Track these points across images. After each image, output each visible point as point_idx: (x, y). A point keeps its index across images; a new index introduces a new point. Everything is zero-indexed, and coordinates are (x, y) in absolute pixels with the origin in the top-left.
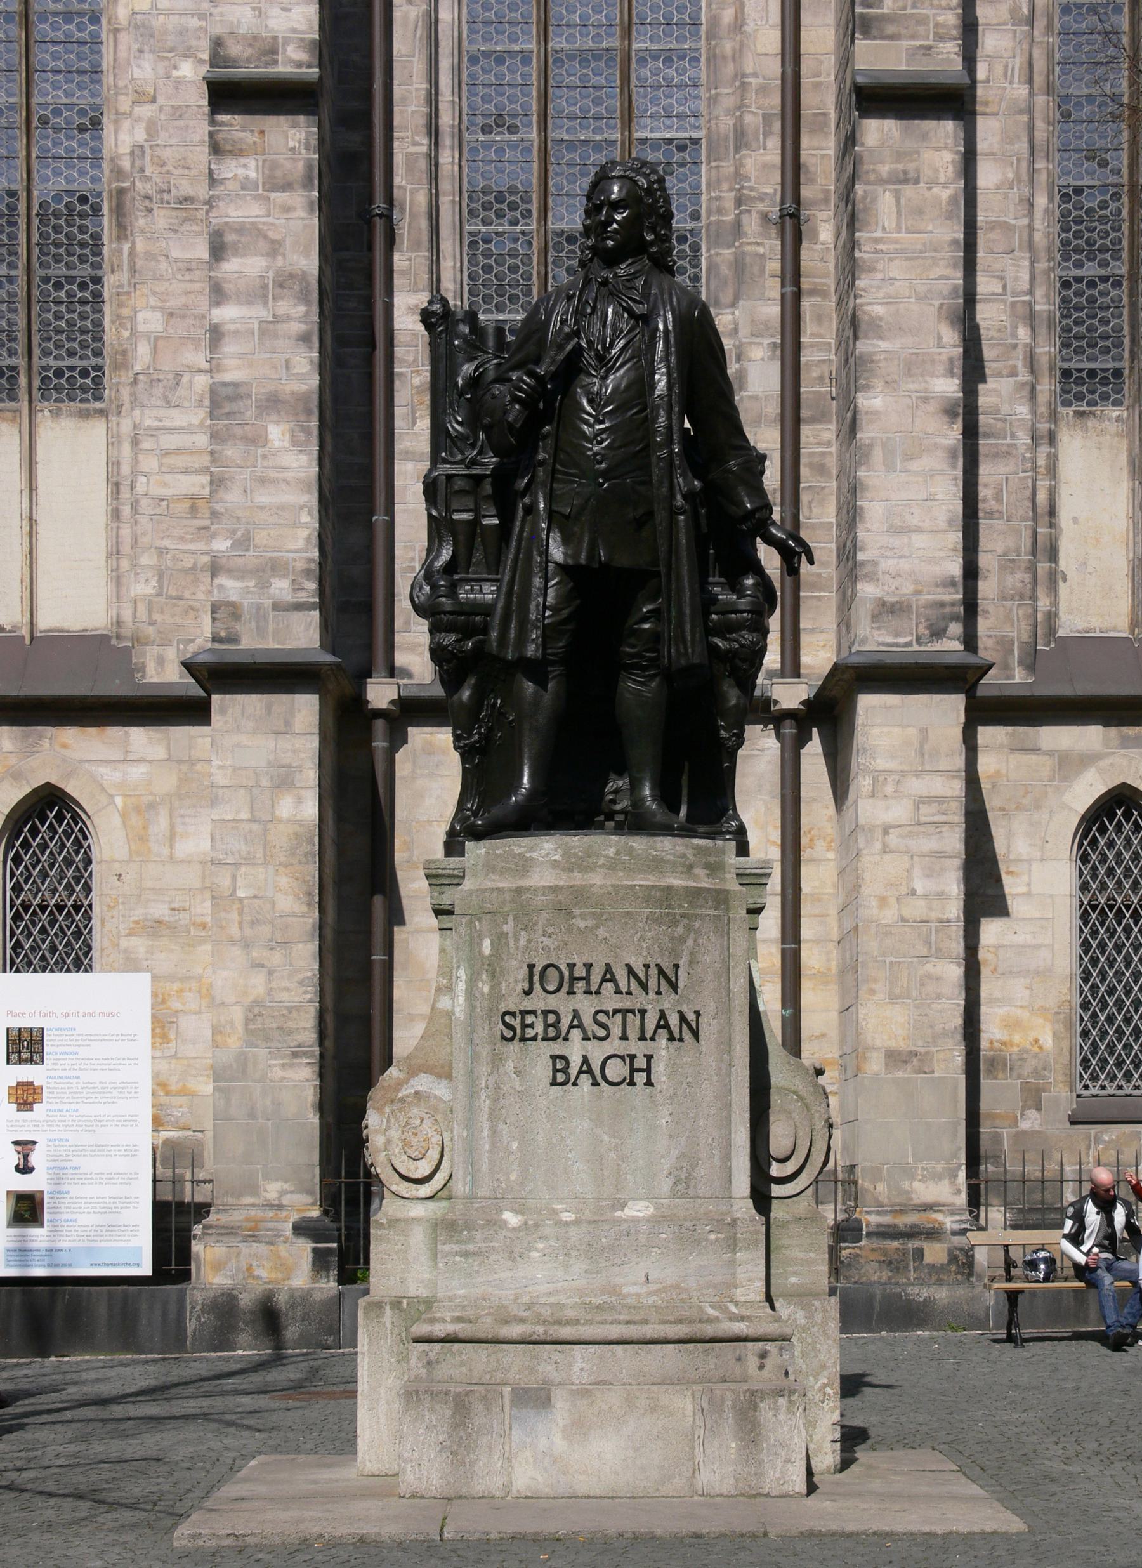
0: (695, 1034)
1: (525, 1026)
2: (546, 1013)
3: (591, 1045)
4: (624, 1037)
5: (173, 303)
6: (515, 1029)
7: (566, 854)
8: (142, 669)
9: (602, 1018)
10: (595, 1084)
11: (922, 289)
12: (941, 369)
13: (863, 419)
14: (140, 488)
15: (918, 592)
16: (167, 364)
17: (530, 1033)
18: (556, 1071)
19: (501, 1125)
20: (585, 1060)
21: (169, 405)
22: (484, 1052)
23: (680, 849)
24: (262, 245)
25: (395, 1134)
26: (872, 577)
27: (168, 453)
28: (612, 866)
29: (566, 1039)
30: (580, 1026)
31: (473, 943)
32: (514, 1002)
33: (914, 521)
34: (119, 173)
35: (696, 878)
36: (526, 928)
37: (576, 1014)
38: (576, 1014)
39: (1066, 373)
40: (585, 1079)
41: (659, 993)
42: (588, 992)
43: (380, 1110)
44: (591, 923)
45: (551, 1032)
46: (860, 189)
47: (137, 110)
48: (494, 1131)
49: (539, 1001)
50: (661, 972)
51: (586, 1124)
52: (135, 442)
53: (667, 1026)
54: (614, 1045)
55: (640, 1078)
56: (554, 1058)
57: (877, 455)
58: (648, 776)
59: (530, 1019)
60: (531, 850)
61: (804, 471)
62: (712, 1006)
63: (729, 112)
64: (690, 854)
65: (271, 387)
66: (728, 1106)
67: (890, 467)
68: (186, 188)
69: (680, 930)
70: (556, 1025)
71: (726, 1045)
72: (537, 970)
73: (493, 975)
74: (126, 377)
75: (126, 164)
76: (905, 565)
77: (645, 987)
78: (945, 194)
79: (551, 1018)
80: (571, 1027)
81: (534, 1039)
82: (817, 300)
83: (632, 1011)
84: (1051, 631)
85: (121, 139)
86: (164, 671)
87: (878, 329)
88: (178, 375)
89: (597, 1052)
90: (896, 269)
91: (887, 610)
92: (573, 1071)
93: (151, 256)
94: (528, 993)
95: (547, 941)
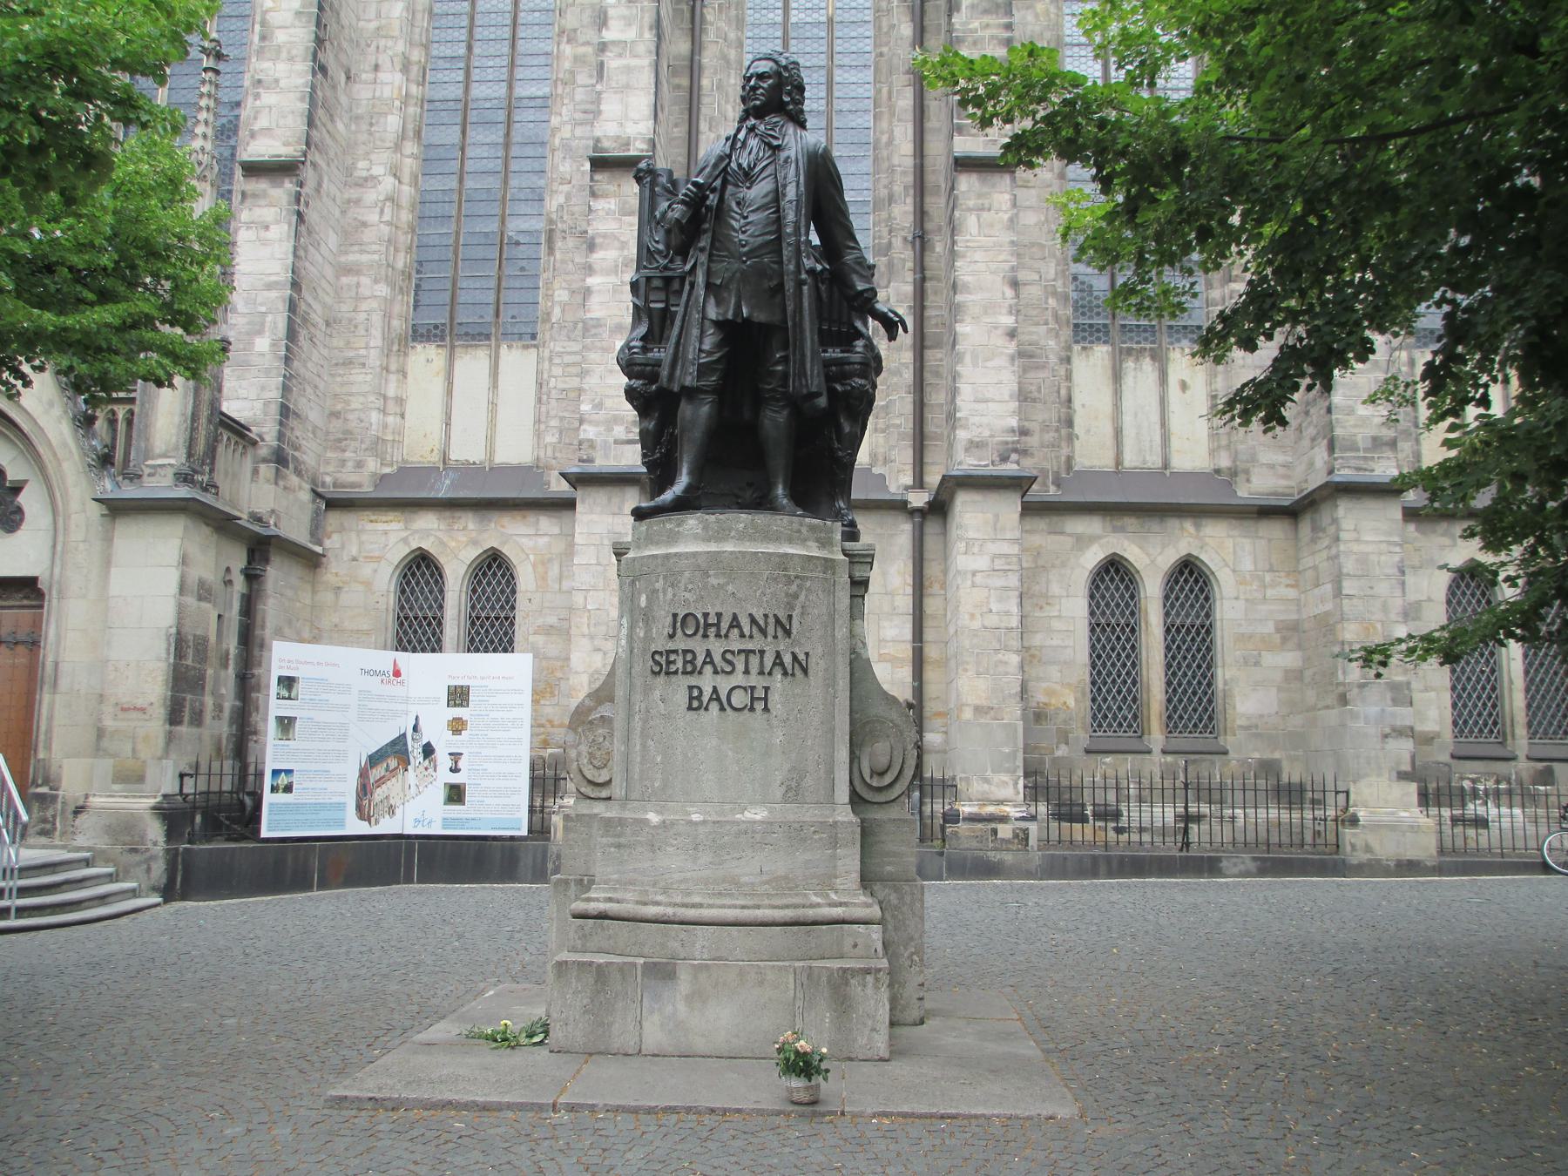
0: (805, 671)
1: (669, 663)
2: (685, 652)
3: (719, 678)
4: (747, 672)
5: (575, 286)
6: (662, 665)
7: (705, 528)
8: (548, 484)
9: (729, 656)
10: (722, 709)
11: (993, 266)
12: (1004, 311)
13: (960, 338)
14: (552, 385)
15: (992, 436)
16: (569, 317)
17: (673, 668)
18: (691, 698)
19: (650, 742)
20: (715, 690)
21: (569, 339)
22: (638, 682)
23: (796, 526)
24: (616, 244)
25: (584, 748)
26: (966, 427)
27: (568, 365)
28: (742, 536)
29: (700, 673)
30: (712, 662)
31: (633, 598)
32: (661, 644)
33: (989, 396)
34: (551, 222)
35: (808, 548)
36: (672, 585)
37: (708, 654)
38: (708, 654)
39: (1076, 326)
40: (714, 706)
41: (775, 637)
42: (718, 635)
43: (575, 730)
44: (721, 581)
45: (689, 668)
46: (957, 214)
47: (561, 188)
48: (644, 746)
49: (680, 643)
50: (778, 621)
51: (715, 742)
52: (551, 360)
53: (782, 664)
54: (738, 679)
55: (759, 706)
56: (691, 688)
57: (968, 359)
58: (781, 480)
59: (672, 657)
60: (679, 525)
61: (927, 375)
62: (820, 650)
63: (885, 187)
64: (804, 530)
65: (617, 320)
66: (832, 730)
67: (975, 365)
68: (584, 226)
69: (794, 588)
70: (692, 662)
71: (830, 682)
72: (679, 619)
73: (647, 623)
74: (548, 326)
75: (554, 216)
76: (985, 420)
77: (764, 632)
78: (1006, 217)
79: (689, 657)
80: (705, 663)
81: (676, 672)
82: (934, 283)
83: (753, 652)
84: (1069, 467)
85: (553, 203)
86: (560, 487)
87: (967, 288)
88: (576, 323)
89: (724, 684)
90: (978, 256)
91: (975, 445)
92: (705, 699)
93: (563, 261)
94: (672, 636)
95: (687, 595)
